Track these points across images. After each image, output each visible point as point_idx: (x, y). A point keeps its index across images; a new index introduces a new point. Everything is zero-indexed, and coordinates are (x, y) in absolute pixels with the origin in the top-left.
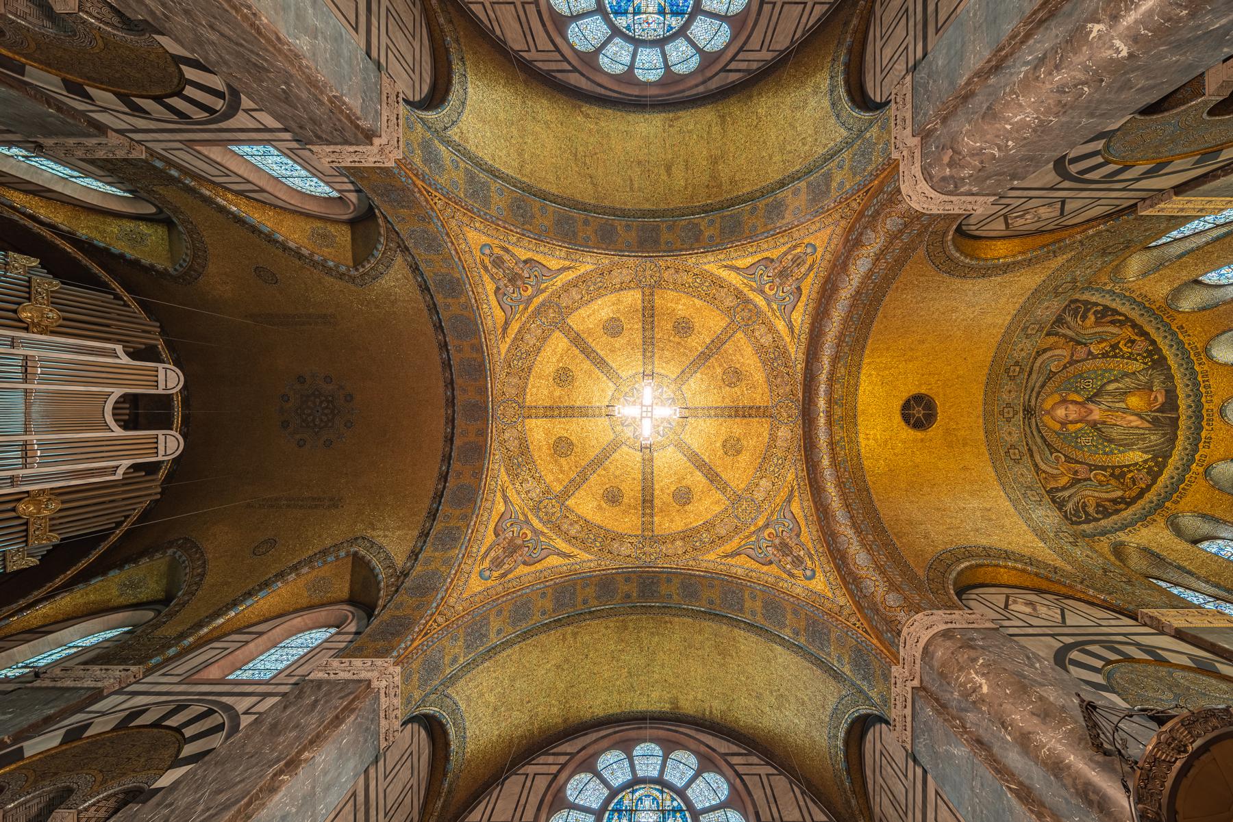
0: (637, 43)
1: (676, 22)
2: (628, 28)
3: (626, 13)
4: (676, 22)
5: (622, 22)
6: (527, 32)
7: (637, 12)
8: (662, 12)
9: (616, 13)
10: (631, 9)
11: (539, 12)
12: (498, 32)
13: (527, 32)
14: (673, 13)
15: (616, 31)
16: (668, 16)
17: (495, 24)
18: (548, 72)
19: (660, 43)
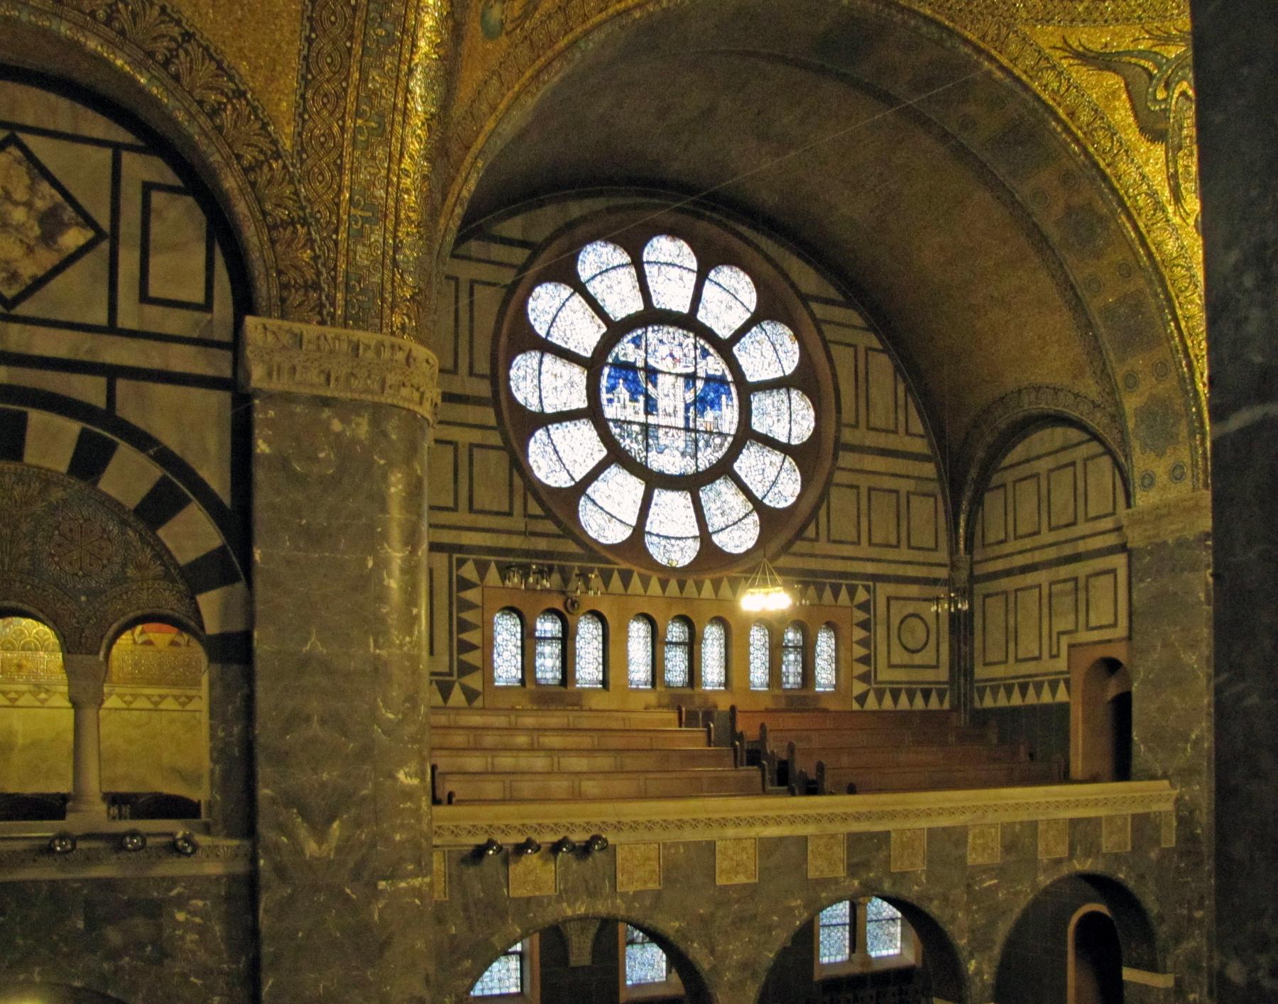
0: (688, 322)
1: (626, 350)
2: (705, 354)
3: (709, 379)
4: (626, 350)
5: (715, 365)
6: (862, 380)
7: (690, 378)
8: (652, 373)
9: (721, 381)
10: (700, 384)
11: (839, 411)
12: (901, 387)
13: (862, 380)
14: (631, 367)
15: (724, 348)
16: (640, 364)
17: (901, 402)
18: (847, 304)
19: (652, 316)
